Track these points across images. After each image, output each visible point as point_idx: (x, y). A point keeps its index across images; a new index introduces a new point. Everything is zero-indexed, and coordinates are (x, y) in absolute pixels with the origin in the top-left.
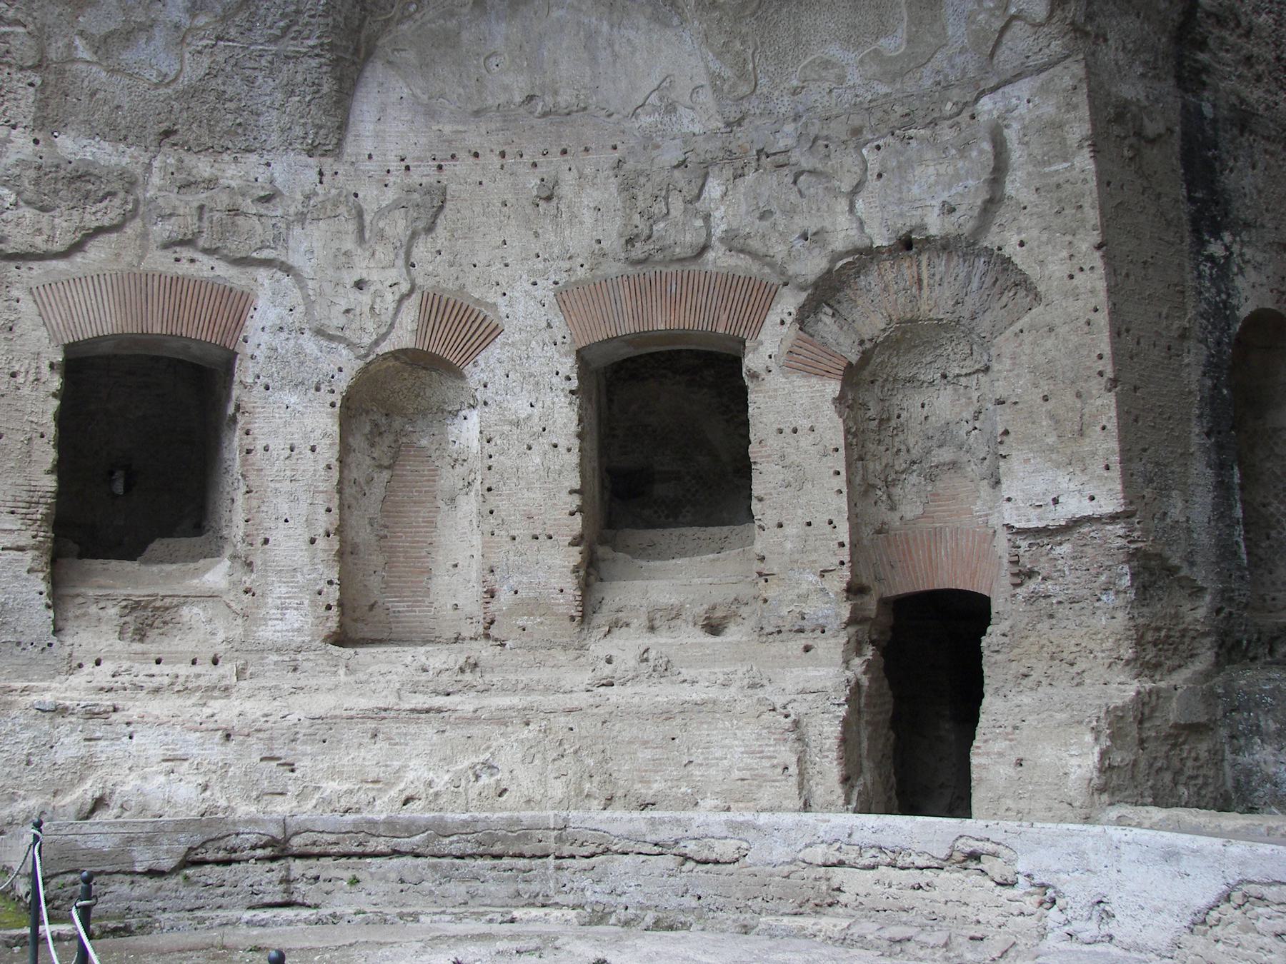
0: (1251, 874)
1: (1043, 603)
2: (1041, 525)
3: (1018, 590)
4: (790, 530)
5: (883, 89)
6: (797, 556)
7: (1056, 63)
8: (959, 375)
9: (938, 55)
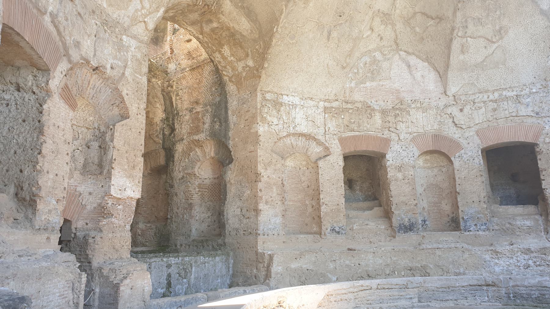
4: (51, 176)
8: (75, 125)
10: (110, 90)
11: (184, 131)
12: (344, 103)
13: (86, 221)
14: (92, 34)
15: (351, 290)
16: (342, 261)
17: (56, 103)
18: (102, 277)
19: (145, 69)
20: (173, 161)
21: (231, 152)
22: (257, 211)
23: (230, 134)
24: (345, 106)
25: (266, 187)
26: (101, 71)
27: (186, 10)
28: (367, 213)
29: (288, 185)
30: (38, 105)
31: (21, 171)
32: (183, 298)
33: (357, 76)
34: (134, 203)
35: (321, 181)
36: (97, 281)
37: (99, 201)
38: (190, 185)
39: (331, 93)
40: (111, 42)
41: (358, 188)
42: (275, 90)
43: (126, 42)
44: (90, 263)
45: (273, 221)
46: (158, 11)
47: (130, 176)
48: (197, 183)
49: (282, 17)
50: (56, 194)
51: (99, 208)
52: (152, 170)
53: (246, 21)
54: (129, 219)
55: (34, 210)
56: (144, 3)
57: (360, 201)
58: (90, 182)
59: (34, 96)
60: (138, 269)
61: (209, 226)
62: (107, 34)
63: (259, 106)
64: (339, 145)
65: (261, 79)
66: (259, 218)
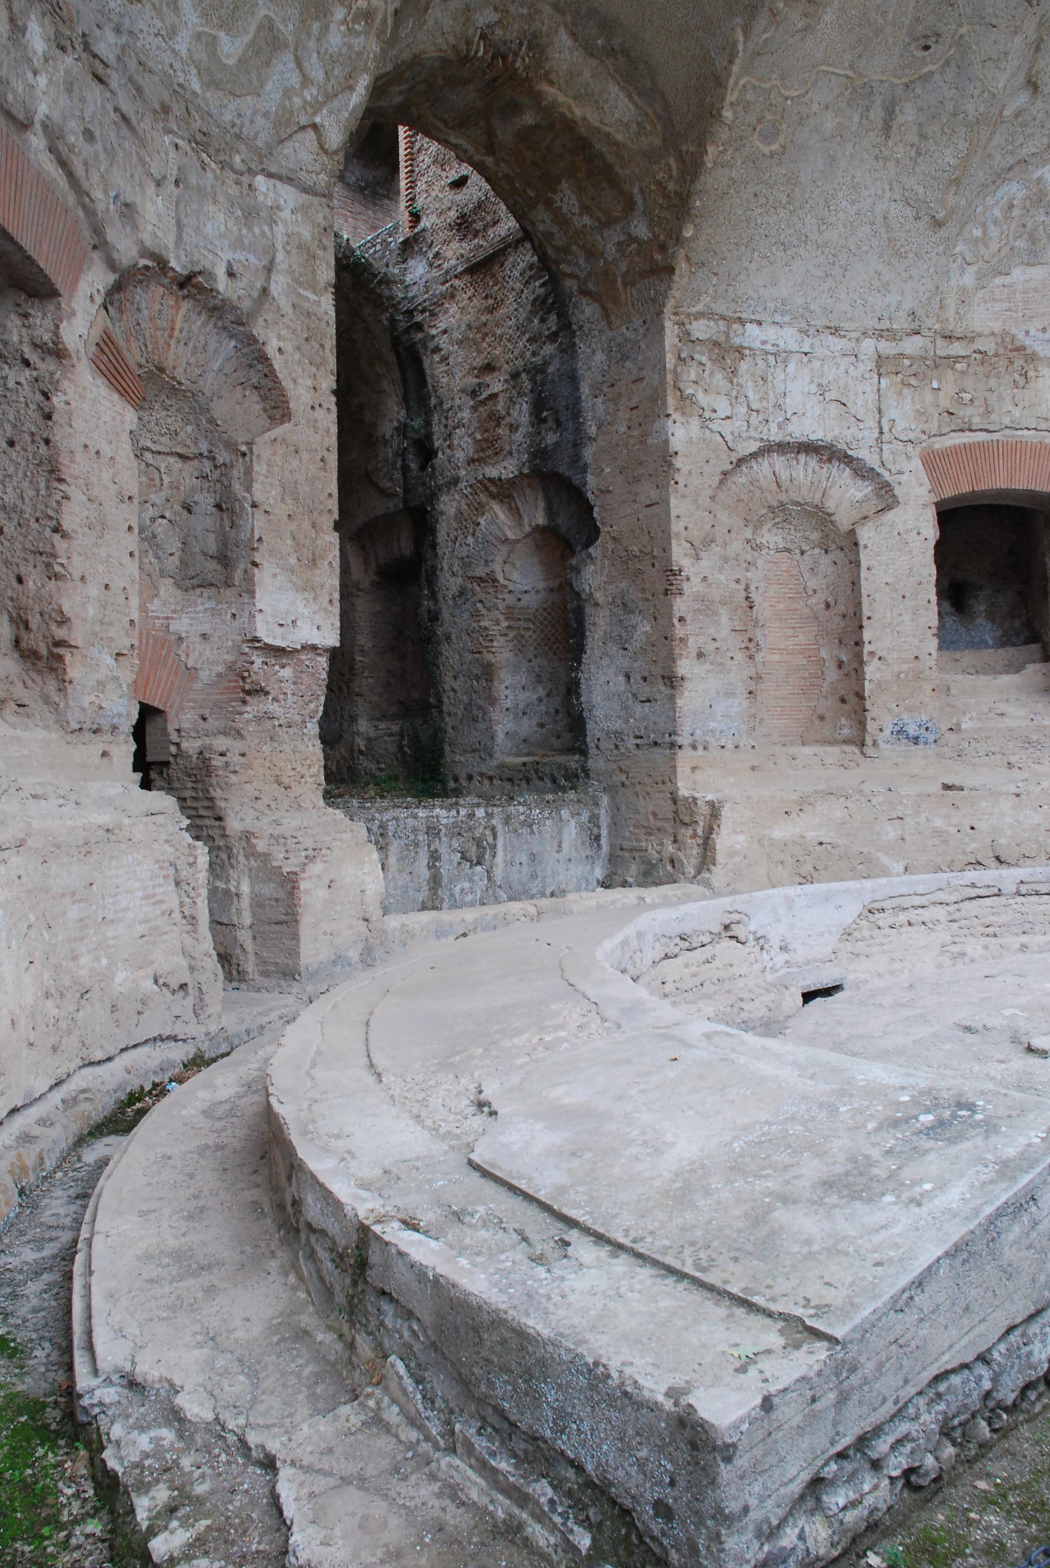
0: (878, 897)
1: (268, 724)
2: (283, 645)
3: (248, 709)
4: (93, 590)
5: (196, 86)
6: (97, 628)
7: (316, 194)
8: (148, 449)
9: (249, 99)
10: (233, 343)
11: (460, 455)
12: (939, 342)
13: (201, 711)
14: (165, 177)
15: (941, 896)
16: (922, 819)
17: (84, 388)
18: (253, 855)
19: (327, 273)
20: (434, 546)
21: (592, 508)
22: (671, 681)
23: (588, 453)
24: (943, 349)
25: (697, 611)
26: (200, 289)
27: (440, 81)
28: (1005, 679)
29: (766, 604)
30: (39, 397)
31: (20, 580)
32: (470, 915)
33: (983, 250)
34: (323, 662)
35: (865, 588)
36: (241, 866)
37: (229, 658)
38: (484, 612)
39: (898, 308)
40: (221, 199)
41: (983, 607)
42: (721, 308)
43: (266, 196)
44: (219, 819)
45: (719, 709)
46: (351, 88)
47: (308, 588)
48: (501, 605)
49: (735, 68)
50: (111, 639)
51: (231, 676)
52: (381, 572)
53: (621, 95)
54: (312, 706)
55: (63, 683)
56: (306, 65)
57: (987, 646)
58: (201, 608)
59: (27, 372)
60: (344, 836)
61: (542, 726)
62: (210, 175)
63: (670, 361)
64: (922, 474)
65: (676, 278)
66: (680, 702)
